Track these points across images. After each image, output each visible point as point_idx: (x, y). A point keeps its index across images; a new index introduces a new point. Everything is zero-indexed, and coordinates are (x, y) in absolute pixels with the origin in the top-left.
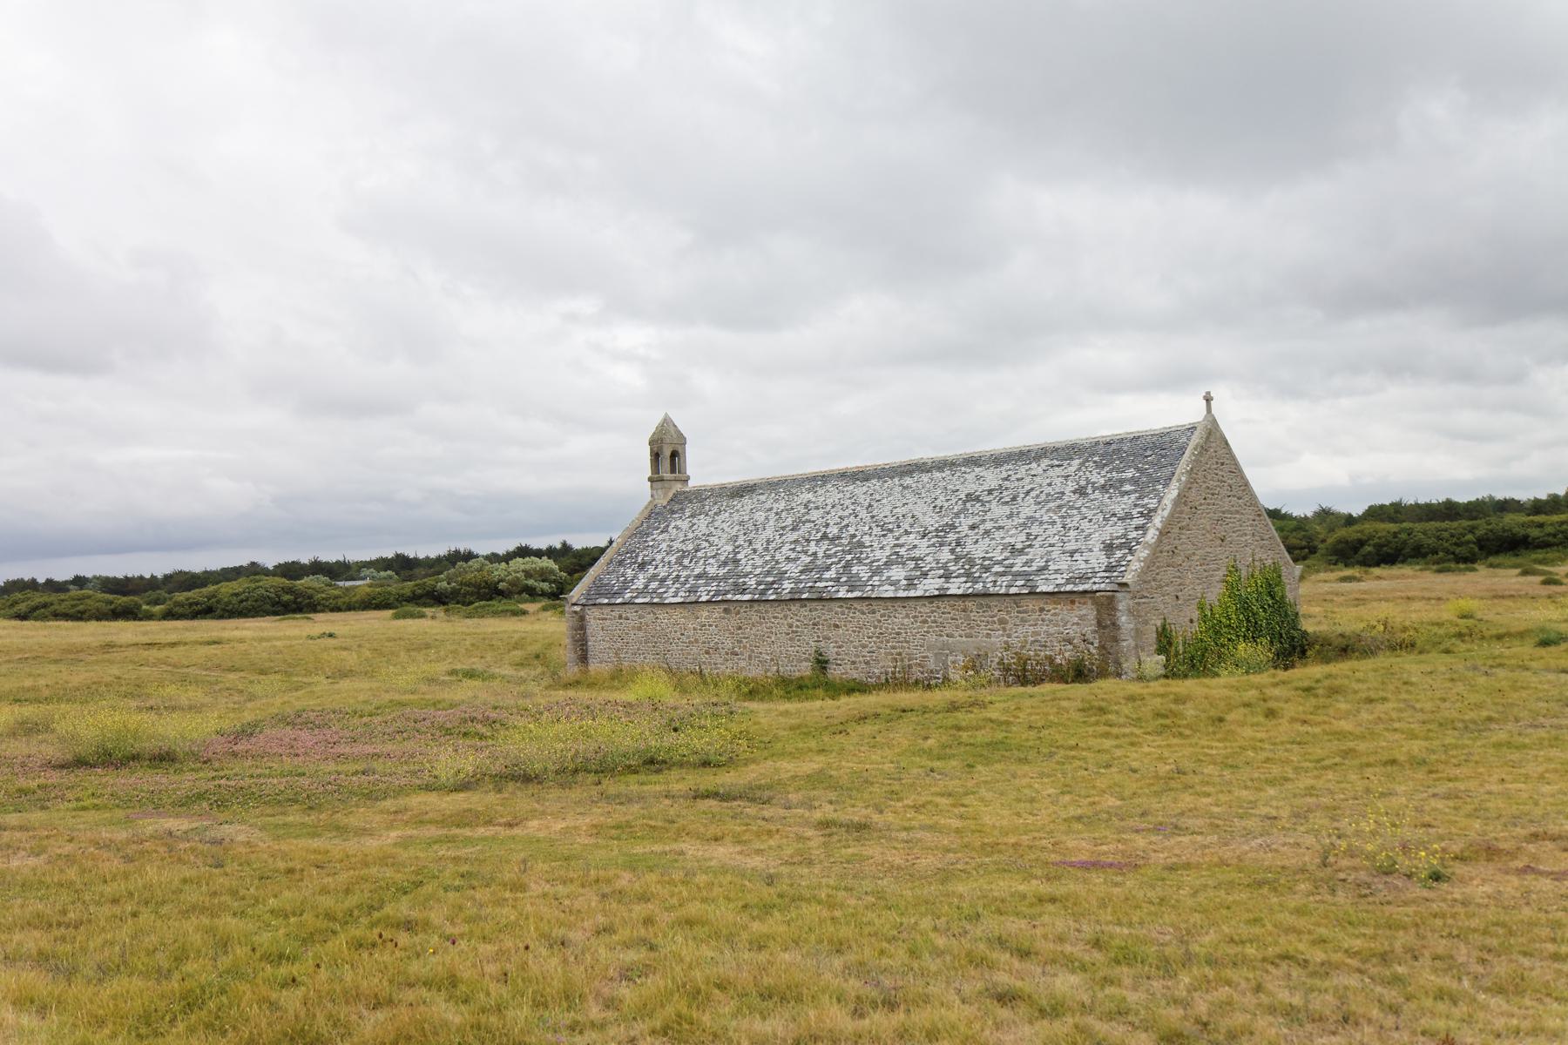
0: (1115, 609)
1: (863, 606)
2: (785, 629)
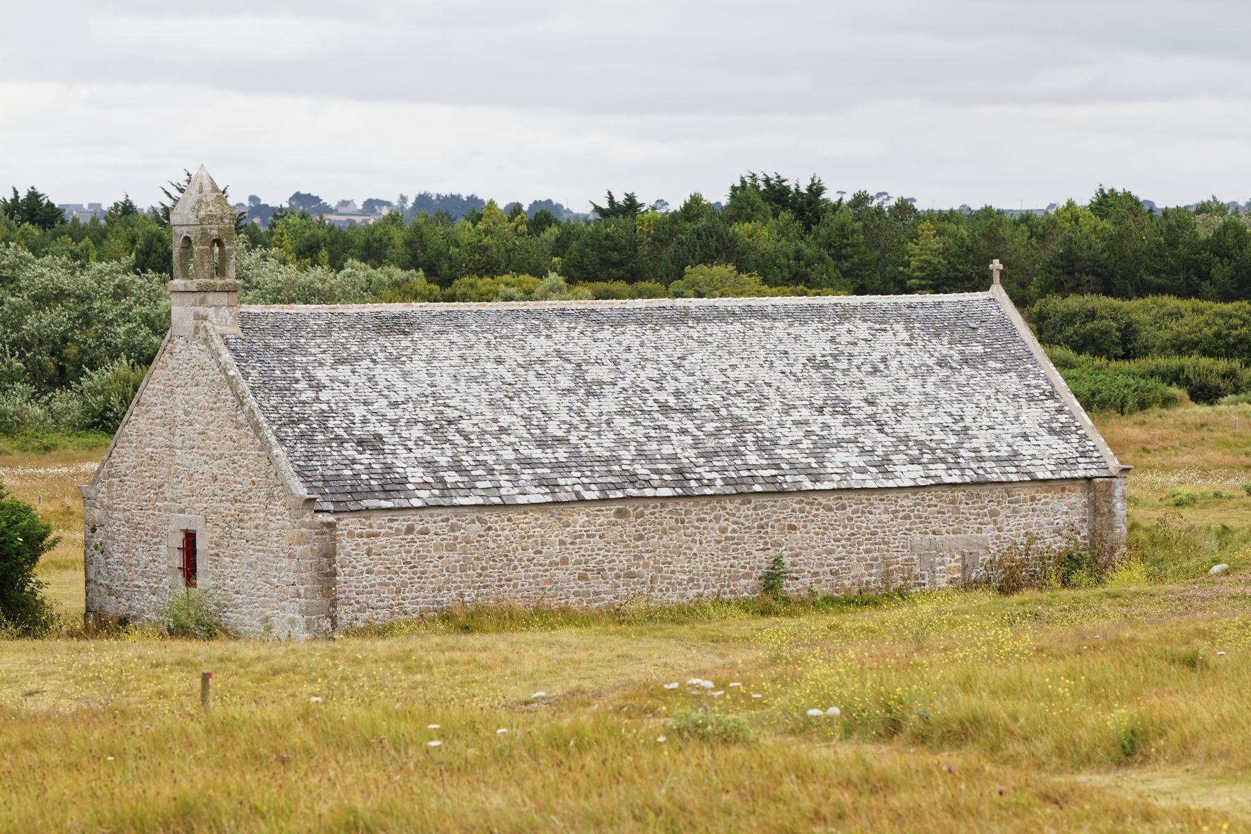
0: (1112, 496)
1: (831, 501)
2: (716, 535)
